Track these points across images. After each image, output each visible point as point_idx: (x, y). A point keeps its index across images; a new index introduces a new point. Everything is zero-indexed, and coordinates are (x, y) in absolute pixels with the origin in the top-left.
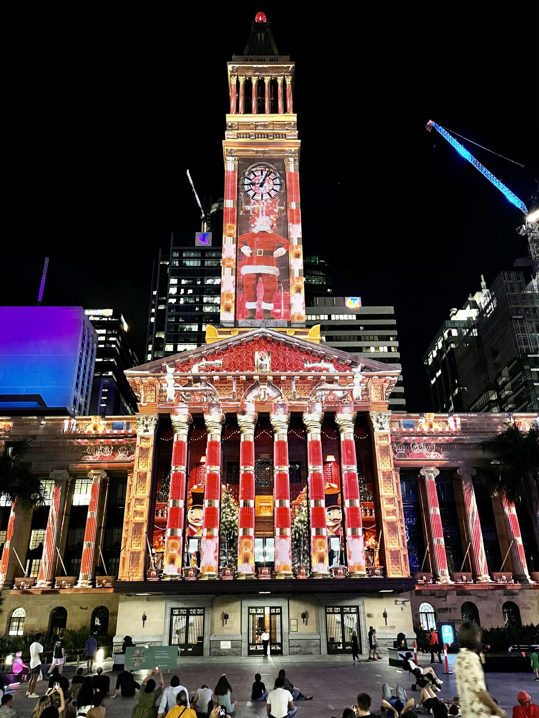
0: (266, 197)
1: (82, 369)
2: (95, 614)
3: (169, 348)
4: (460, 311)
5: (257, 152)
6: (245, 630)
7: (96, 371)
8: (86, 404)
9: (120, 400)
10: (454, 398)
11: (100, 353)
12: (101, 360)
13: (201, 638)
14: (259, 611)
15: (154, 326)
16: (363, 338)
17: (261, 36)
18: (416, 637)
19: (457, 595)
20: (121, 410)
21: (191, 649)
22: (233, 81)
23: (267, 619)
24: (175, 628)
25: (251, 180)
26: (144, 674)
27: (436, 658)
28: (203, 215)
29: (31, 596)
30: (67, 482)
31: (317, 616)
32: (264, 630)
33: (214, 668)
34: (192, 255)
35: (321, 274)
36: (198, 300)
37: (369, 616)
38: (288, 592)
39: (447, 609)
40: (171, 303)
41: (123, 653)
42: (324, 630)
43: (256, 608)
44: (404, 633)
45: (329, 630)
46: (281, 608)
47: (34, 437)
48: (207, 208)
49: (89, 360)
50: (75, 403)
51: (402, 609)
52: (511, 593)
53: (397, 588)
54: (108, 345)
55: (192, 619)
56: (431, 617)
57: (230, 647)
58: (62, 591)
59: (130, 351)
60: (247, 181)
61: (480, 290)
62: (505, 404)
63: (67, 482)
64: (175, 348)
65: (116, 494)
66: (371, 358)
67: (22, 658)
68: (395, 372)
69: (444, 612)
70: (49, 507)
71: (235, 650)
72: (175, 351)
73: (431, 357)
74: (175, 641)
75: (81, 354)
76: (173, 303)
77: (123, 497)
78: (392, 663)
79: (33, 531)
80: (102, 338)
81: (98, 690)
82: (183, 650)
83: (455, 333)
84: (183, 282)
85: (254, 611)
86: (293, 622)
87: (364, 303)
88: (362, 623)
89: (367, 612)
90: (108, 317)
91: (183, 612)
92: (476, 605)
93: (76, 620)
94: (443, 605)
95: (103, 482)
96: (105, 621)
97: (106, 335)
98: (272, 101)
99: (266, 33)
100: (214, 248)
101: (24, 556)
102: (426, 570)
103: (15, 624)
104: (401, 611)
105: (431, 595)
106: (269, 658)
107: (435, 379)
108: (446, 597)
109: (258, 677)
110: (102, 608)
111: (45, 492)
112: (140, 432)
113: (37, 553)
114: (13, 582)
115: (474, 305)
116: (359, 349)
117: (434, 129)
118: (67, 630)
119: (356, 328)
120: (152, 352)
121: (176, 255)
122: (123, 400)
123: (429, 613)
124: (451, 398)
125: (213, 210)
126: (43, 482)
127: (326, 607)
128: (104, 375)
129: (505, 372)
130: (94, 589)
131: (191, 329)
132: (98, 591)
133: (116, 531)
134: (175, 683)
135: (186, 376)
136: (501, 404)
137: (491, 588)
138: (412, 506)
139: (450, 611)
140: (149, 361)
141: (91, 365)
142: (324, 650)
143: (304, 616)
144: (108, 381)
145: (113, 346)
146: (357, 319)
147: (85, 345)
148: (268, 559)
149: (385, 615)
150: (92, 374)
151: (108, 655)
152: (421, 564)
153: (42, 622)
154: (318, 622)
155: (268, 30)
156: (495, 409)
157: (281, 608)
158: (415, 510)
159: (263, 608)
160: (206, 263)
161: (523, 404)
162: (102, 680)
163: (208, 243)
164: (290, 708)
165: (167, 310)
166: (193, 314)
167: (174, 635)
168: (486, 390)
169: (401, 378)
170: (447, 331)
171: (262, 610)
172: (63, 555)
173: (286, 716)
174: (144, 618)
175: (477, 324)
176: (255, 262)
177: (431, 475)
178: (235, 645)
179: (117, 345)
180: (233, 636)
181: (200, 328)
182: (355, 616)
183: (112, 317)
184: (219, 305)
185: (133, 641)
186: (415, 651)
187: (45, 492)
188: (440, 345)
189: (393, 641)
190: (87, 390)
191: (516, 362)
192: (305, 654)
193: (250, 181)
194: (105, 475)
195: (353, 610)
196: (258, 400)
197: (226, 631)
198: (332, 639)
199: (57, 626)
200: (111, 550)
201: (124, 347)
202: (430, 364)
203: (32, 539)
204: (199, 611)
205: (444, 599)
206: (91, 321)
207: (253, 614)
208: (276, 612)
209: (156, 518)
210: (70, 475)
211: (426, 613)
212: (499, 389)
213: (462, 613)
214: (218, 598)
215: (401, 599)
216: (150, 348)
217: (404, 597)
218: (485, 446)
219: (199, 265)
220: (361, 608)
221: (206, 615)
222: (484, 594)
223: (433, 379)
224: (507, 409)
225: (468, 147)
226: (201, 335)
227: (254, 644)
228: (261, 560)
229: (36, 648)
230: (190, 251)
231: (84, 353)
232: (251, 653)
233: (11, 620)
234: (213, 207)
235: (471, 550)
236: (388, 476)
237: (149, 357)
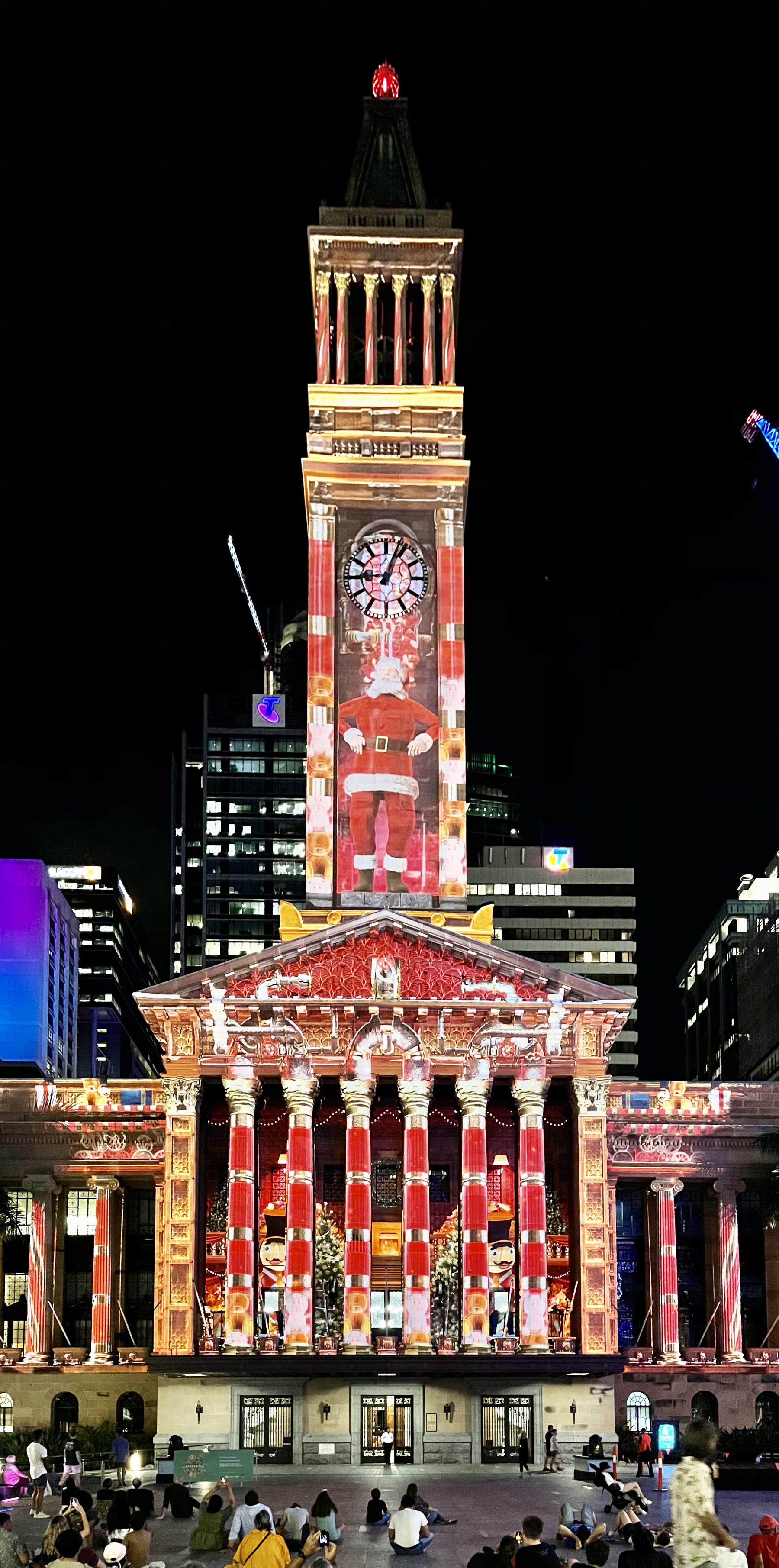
0: (395, 609)
1: (56, 988)
3: (213, 948)
4: (758, 880)
5: (376, 491)
6: (356, 1428)
7: (82, 993)
9: (130, 1048)
11: (87, 957)
12: (88, 971)
13: (288, 1440)
14: (378, 1401)
15: (183, 903)
16: (571, 933)
17: (385, 144)
18: (618, 1441)
19: (689, 1381)
20: (135, 1069)
21: (274, 1455)
22: (321, 286)
23: (390, 1413)
24: (247, 1425)
25: (363, 565)
26: (204, 1488)
27: (646, 1469)
28: (266, 653)
29: (17, 1376)
30: (54, 1196)
31: (468, 1410)
32: (385, 1429)
33: (310, 1481)
34: (248, 747)
35: (500, 795)
36: (262, 848)
37: (549, 1410)
38: (423, 1375)
39: (670, 1401)
40: (211, 855)
41: (171, 1458)
42: (478, 1430)
43: (373, 1397)
44: (600, 1435)
45: (485, 1430)
46: (411, 1397)
48: (274, 636)
49: (67, 970)
50: (50, 1054)
51: (600, 1401)
53: (596, 1370)
54: (99, 943)
55: (273, 1412)
56: (644, 1414)
57: (333, 1452)
58: (65, 1369)
59: (141, 953)
60: (355, 569)
63: (54, 1196)
64: (224, 948)
65: (139, 1218)
66: (582, 975)
67: (16, 1464)
68: (624, 1003)
69: (665, 1405)
70: (27, 1237)
71: (341, 1456)
72: (225, 955)
73: (693, 974)
75: (52, 959)
76: (216, 854)
77: (151, 1222)
78: (579, 1475)
79: (7, 1277)
80: (87, 928)
81: (137, 1509)
82: (262, 1455)
83: (742, 925)
84: (233, 809)
85: (369, 1401)
86: (430, 1418)
88: (537, 1421)
90: (93, 883)
92: (716, 1396)
93: (94, 1411)
94: (665, 1395)
95: (115, 1196)
96: (138, 1413)
98: (409, 346)
99: (397, 135)
100: (291, 732)
102: (644, 1343)
104: (598, 1404)
105: (648, 1381)
106: (393, 1467)
107: (695, 1018)
108: (670, 1384)
109: (376, 1493)
110: (132, 1394)
111: (18, 1213)
112: (171, 1109)
113: (19, 1311)
116: (562, 957)
117: (759, 437)
118: (81, 1427)
119: (559, 912)
120: (182, 957)
121: (215, 746)
122: (136, 1050)
123: (641, 1406)
124: (719, 1054)
125: (287, 641)
127: (482, 1397)
128: (97, 1000)
130: (116, 1367)
131: (252, 910)
132: (124, 1370)
133: (144, 1277)
134: (252, 1499)
135: (247, 1006)
137: (743, 1371)
138: (632, 1243)
139: (674, 1405)
140: (177, 975)
141: (71, 980)
142: (477, 1457)
143: (448, 1409)
144: (106, 1013)
145: (109, 943)
146: (563, 894)
147: (57, 941)
148: (392, 1324)
149: (573, 1409)
150: (75, 998)
151: (148, 1461)
153: (44, 1416)
154: (468, 1418)
155: (403, 124)
157: (411, 1397)
158: (635, 1250)
159: (385, 1397)
160: (275, 766)
162: (141, 1494)
163: (278, 721)
164: (423, 1533)
165: (205, 870)
166: (255, 878)
167: (247, 1434)
169: (635, 1015)
170: (729, 922)
171: (383, 1399)
172: (61, 1314)
173: (417, 1545)
174: (200, 1410)
176: (371, 766)
177: (668, 1191)
178: (340, 1449)
179: (115, 941)
180: (337, 1436)
181: (269, 908)
182: (527, 1410)
183: (101, 882)
184: (303, 861)
185: (183, 1442)
186: (615, 1460)
187: (18, 1213)
189: (582, 1445)
190: (70, 1030)
192: (448, 1462)
193: (360, 569)
194: (116, 1185)
196: (378, 1053)
197: (327, 1430)
198: (490, 1442)
200: (137, 1309)
202: (689, 987)
203: (7, 1288)
204: (284, 1401)
205: (668, 1387)
206: (63, 891)
207: (369, 1406)
208: (404, 1403)
209: (207, 1257)
210: (58, 1184)
211: (637, 1407)
213: (693, 1407)
214: (312, 1382)
215: (599, 1387)
216: (178, 948)
217: (605, 1383)
219: (263, 771)
220: (536, 1400)
221: (296, 1407)
222: (731, 1380)
223: (691, 1017)
226: (271, 924)
227: (370, 1448)
228: (382, 1325)
229: (35, 1451)
230: (243, 737)
231: (57, 957)
232: (364, 1461)
234: (286, 633)
235: (719, 1314)
236: (595, 1192)
237: (178, 966)
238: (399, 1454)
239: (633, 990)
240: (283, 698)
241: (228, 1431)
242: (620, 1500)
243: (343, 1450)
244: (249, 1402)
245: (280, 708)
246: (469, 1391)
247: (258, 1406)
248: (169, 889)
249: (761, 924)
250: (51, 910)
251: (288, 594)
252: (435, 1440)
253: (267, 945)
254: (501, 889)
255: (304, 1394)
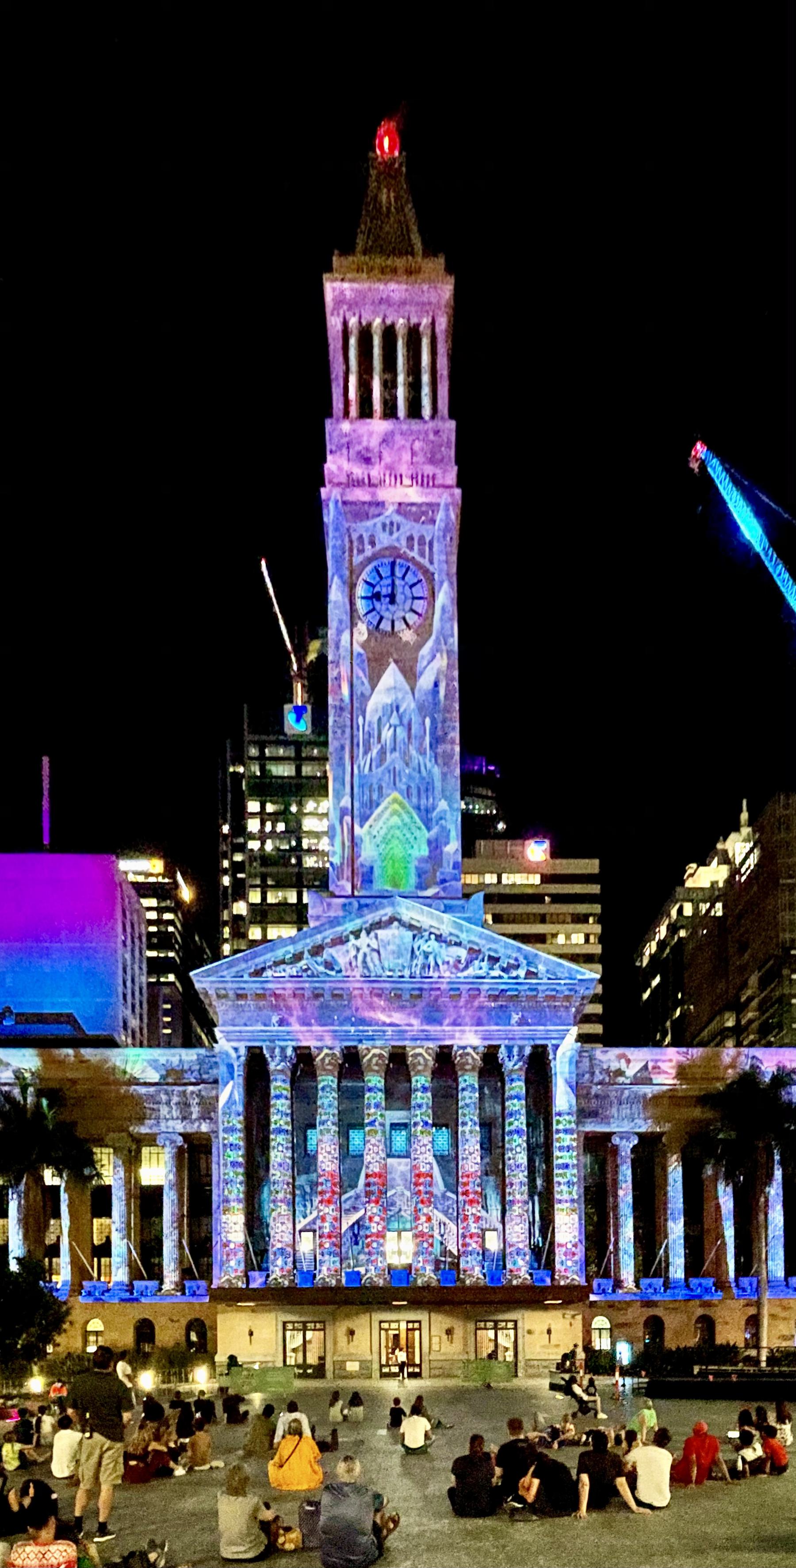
2: (189, 1327)
3: (255, 933)
4: (701, 869)
8: (141, 1029)
10: (672, 1022)
12: (153, 954)
13: (322, 1358)
20: (194, 1040)
23: (403, 1336)
24: (289, 1347)
30: (130, 1151)
31: (465, 1332)
34: (281, 752)
35: (490, 794)
38: (429, 1303)
40: (252, 850)
41: (227, 1374)
42: (473, 1350)
43: (390, 1322)
47: (74, 1082)
48: (301, 650)
51: (571, 1324)
52: (707, 1305)
54: (163, 929)
55: (309, 1335)
56: (606, 1335)
58: (143, 1300)
59: (197, 938)
61: (737, 829)
62: (745, 1034)
72: (265, 940)
73: (647, 953)
74: (291, 1361)
78: (553, 1387)
79: (95, 1220)
80: (152, 915)
84: (270, 808)
85: (385, 1325)
86: (435, 1340)
87: (556, 853)
89: (527, 1327)
90: (157, 875)
91: (300, 1326)
93: (168, 1335)
94: (622, 1319)
95: (180, 1151)
96: (202, 1335)
97: (160, 910)
101: (89, 1252)
102: (606, 1275)
103: (92, 1338)
106: (406, 1381)
110: (197, 1320)
113: (104, 1250)
114: (82, 1287)
115: (726, 860)
116: (541, 939)
117: (703, 465)
119: (537, 898)
121: (254, 752)
122: (194, 1023)
124: (668, 1024)
125: (312, 657)
126: (96, 1150)
128: (162, 980)
129: (753, 980)
130: (184, 1298)
131: (286, 899)
133: (205, 1221)
134: (292, 1407)
136: (738, 1034)
141: (141, 962)
143: (449, 1332)
145: (171, 929)
146: (542, 882)
152: (599, 1269)
153: (126, 1339)
154: (465, 1339)
156: (730, 1043)
157: (419, 1322)
161: (767, 1034)
162: (205, 1405)
165: (247, 864)
167: (289, 1354)
168: (720, 1012)
169: (599, 989)
170: (677, 906)
175: (725, 894)
179: (176, 927)
182: (512, 1332)
187: (102, 1166)
188: (662, 931)
191: (771, 962)
192: (449, 1376)
194: (180, 1141)
195: (510, 1325)
197: (352, 1351)
199: (145, 1341)
201: (187, 931)
202: (644, 964)
204: (318, 1326)
207: (387, 1330)
208: (414, 1327)
212: (739, 1008)
215: (569, 1313)
216: (227, 931)
218: (704, 1100)
220: (520, 1324)
223: (645, 991)
224: (745, 1043)
225: (760, 511)
230: (278, 743)
232: (383, 1376)
233: (86, 1334)
237: (226, 948)
238: (411, 1370)
239: (599, 967)
240: (309, 707)
241: (272, 1351)
242: (584, 1408)
243: (365, 1365)
244: (290, 1326)
245: (307, 716)
246: (467, 1318)
247: (298, 1330)
248: (218, 882)
249: (704, 907)
250: (122, 899)
251: (311, 617)
252: (439, 1358)
253: (300, 929)
254: (490, 879)
255: (335, 1320)
